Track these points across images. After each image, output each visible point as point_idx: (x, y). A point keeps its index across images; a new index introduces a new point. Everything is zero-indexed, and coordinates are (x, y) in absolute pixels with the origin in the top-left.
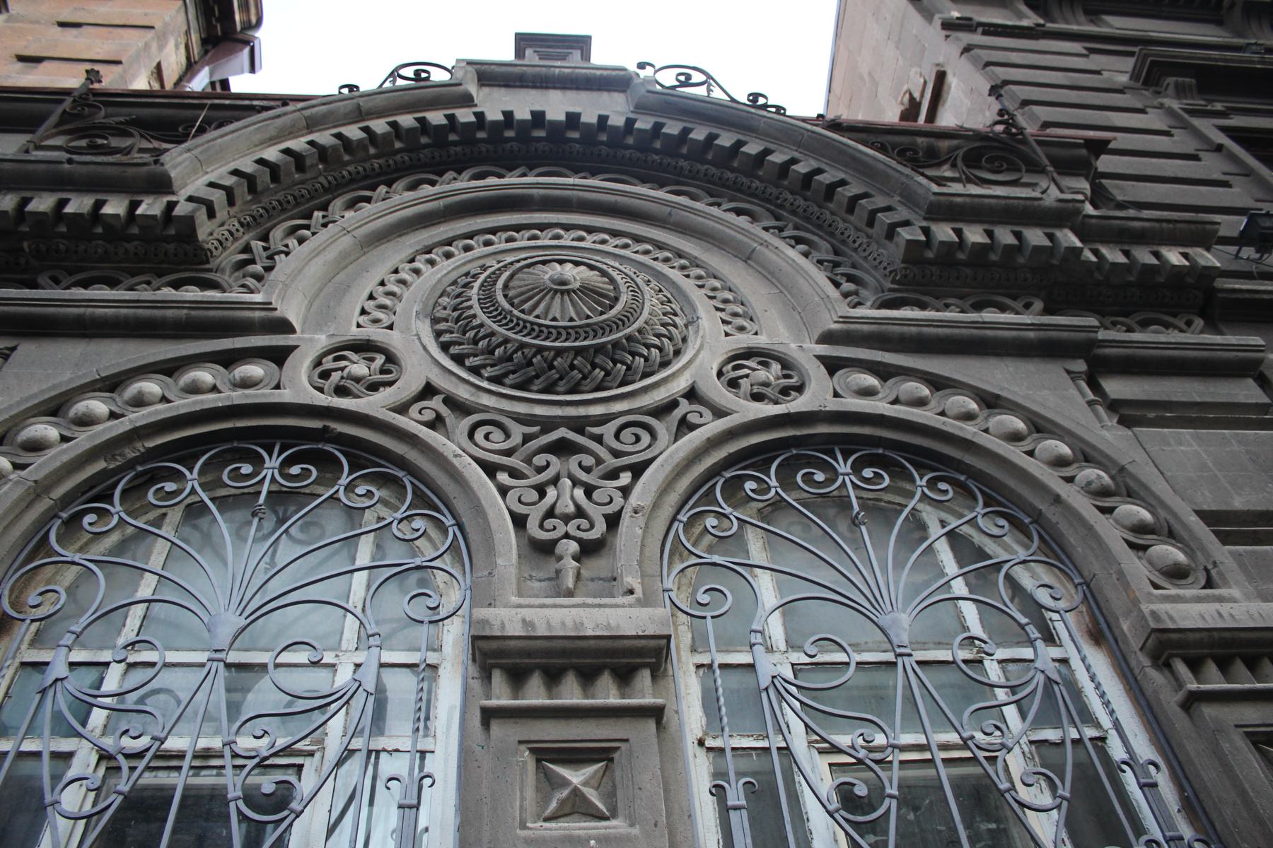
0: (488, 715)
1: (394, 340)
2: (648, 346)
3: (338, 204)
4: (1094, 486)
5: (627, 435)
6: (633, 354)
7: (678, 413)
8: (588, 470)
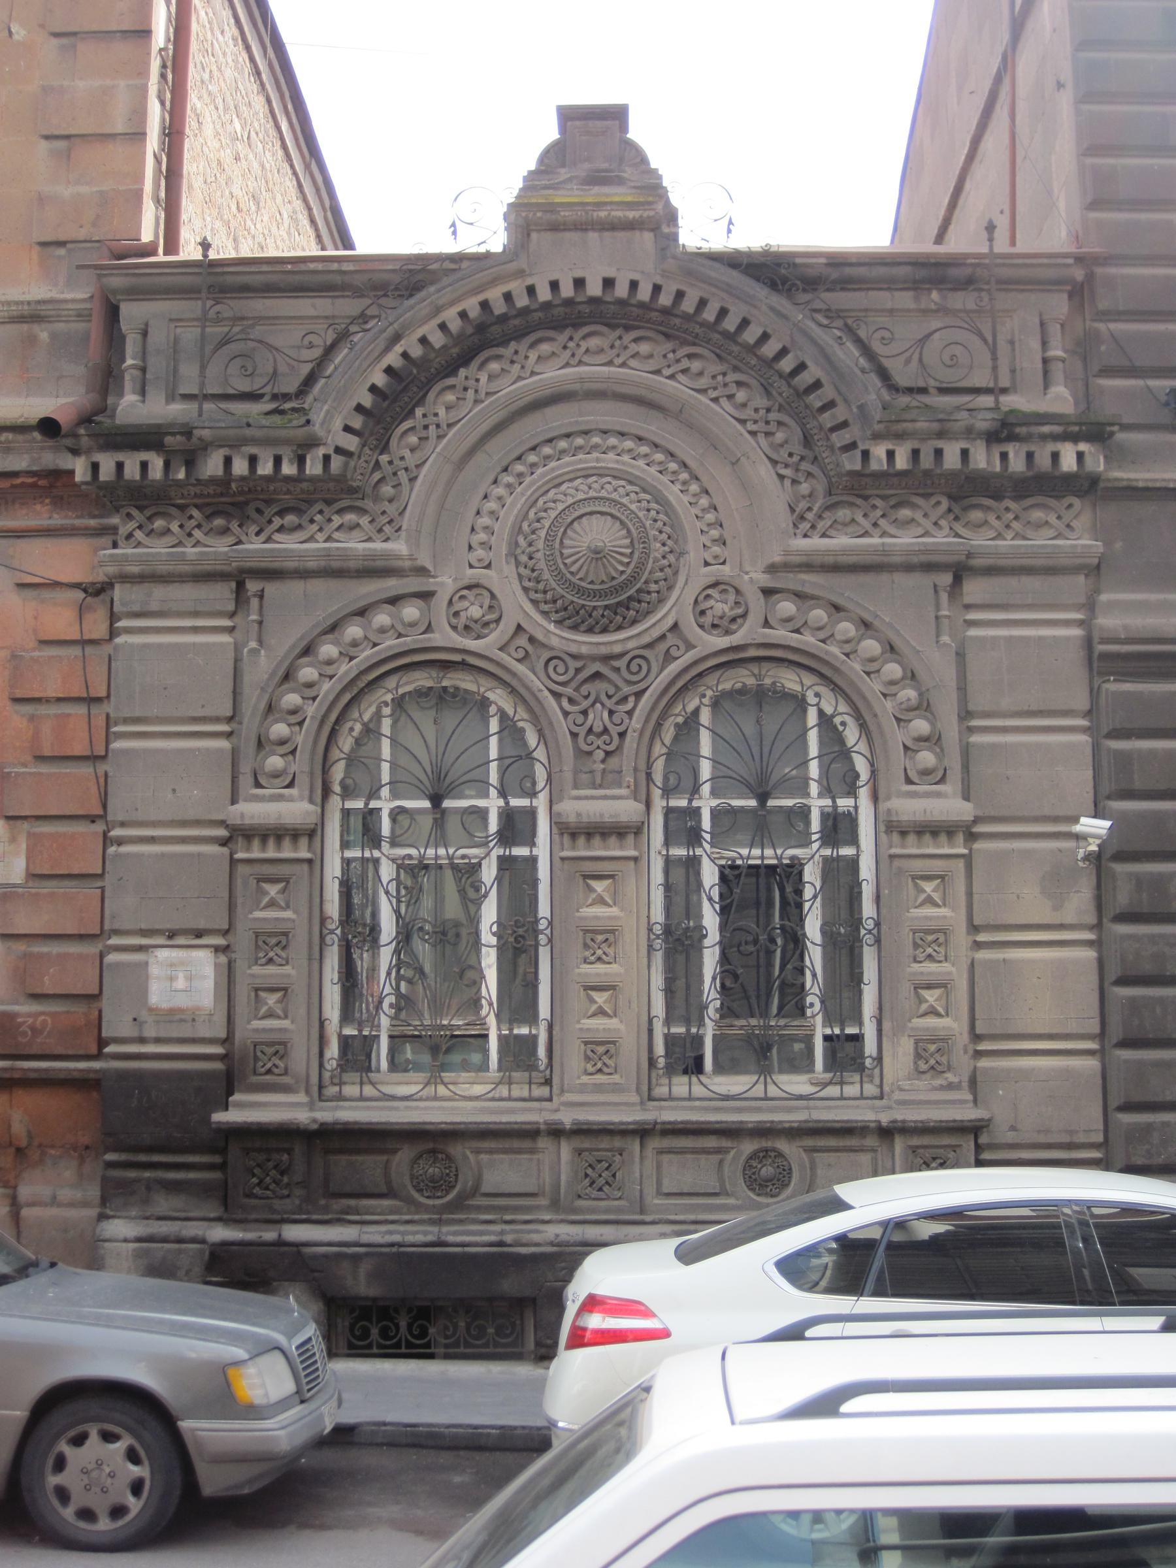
0: (563, 859)
1: (491, 578)
2: (649, 593)
3: (431, 395)
4: (903, 706)
5: (634, 668)
6: (639, 602)
7: (662, 647)
8: (609, 697)
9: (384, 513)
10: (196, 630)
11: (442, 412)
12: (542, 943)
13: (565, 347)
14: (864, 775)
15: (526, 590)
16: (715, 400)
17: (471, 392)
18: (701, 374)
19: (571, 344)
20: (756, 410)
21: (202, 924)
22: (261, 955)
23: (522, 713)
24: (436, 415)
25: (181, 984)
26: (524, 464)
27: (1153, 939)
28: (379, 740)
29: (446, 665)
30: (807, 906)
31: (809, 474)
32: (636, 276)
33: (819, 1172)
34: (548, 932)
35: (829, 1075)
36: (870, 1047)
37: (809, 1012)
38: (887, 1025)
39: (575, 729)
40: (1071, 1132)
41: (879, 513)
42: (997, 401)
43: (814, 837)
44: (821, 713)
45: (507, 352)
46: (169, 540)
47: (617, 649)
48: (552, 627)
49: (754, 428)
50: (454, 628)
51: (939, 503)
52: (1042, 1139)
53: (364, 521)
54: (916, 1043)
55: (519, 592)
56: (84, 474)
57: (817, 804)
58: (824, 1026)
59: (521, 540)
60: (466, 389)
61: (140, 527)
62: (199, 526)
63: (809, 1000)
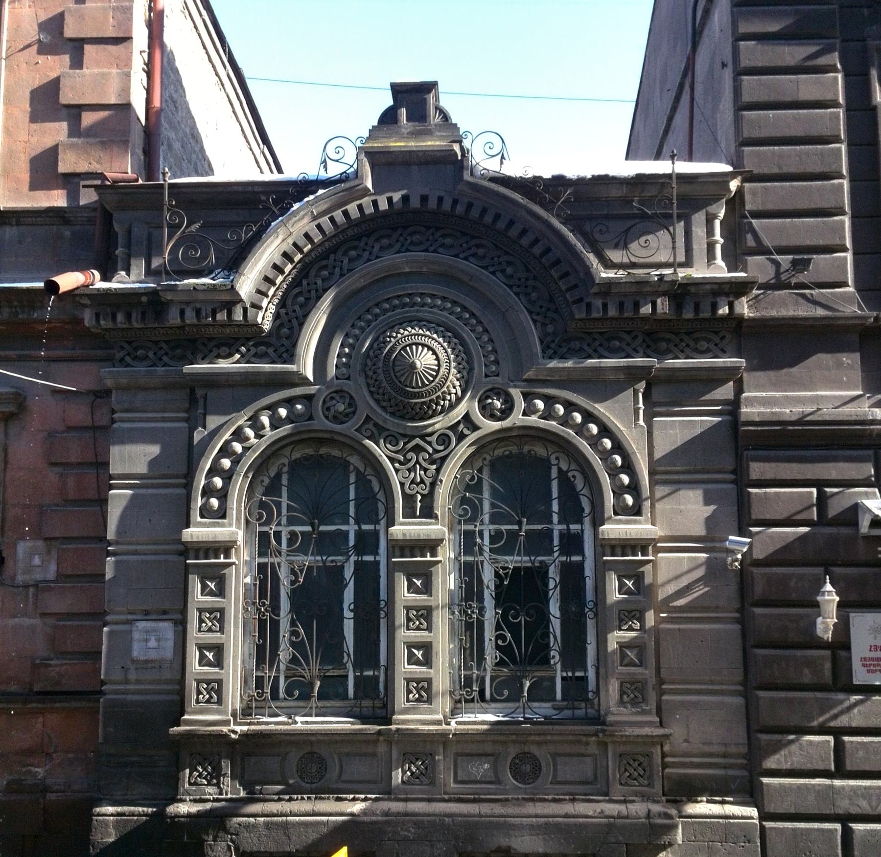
9: (283, 345)
10: (164, 420)
11: (319, 282)
12: (382, 616)
13: (397, 241)
14: (587, 510)
15: (372, 393)
16: (493, 273)
17: (337, 270)
18: (484, 257)
19: (401, 239)
20: (519, 279)
21: (167, 606)
22: (204, 625)
23: (369, 471)
24: (316, 283)
25: (153, 643)
26: (371, 314)
27: (779, 617)
28: (281, 489)
29: (321, 442)
30: (551, 593)
31: (553, 319)
32: (442, 194)
33: (559, 767)
34: (385, 609)
35: (565, 703)
36: (592, 685)
37: (552, 662)
38: (602, 671)
39: (403, 480)
40: (725, 745)
41: (597, 343)
42: (675, 270)
43: (556, 549)
44: (560, 470)
45: (362, 244)
46: (148, 363)
47: (430, 430)
48: (388, 417)
49: (518, 290)
50: (327, 417)
51: (636, 336)
52: (707, 749)
53: (270, 351)
54: (622, 683)
55: (367, 394)
56: (91, 320)
57: (557, 528)
58: (562, 671)
59: (369, 363)
60: (334, 267)
61: (129, 355)
62: (166, 354)
63: (552, 653)
